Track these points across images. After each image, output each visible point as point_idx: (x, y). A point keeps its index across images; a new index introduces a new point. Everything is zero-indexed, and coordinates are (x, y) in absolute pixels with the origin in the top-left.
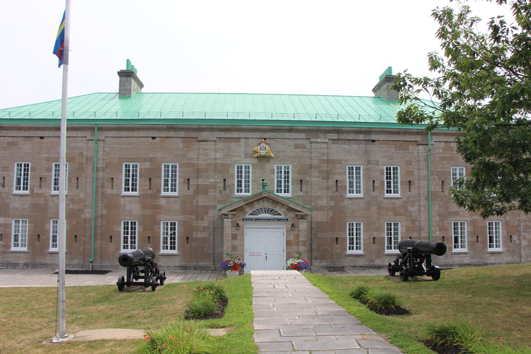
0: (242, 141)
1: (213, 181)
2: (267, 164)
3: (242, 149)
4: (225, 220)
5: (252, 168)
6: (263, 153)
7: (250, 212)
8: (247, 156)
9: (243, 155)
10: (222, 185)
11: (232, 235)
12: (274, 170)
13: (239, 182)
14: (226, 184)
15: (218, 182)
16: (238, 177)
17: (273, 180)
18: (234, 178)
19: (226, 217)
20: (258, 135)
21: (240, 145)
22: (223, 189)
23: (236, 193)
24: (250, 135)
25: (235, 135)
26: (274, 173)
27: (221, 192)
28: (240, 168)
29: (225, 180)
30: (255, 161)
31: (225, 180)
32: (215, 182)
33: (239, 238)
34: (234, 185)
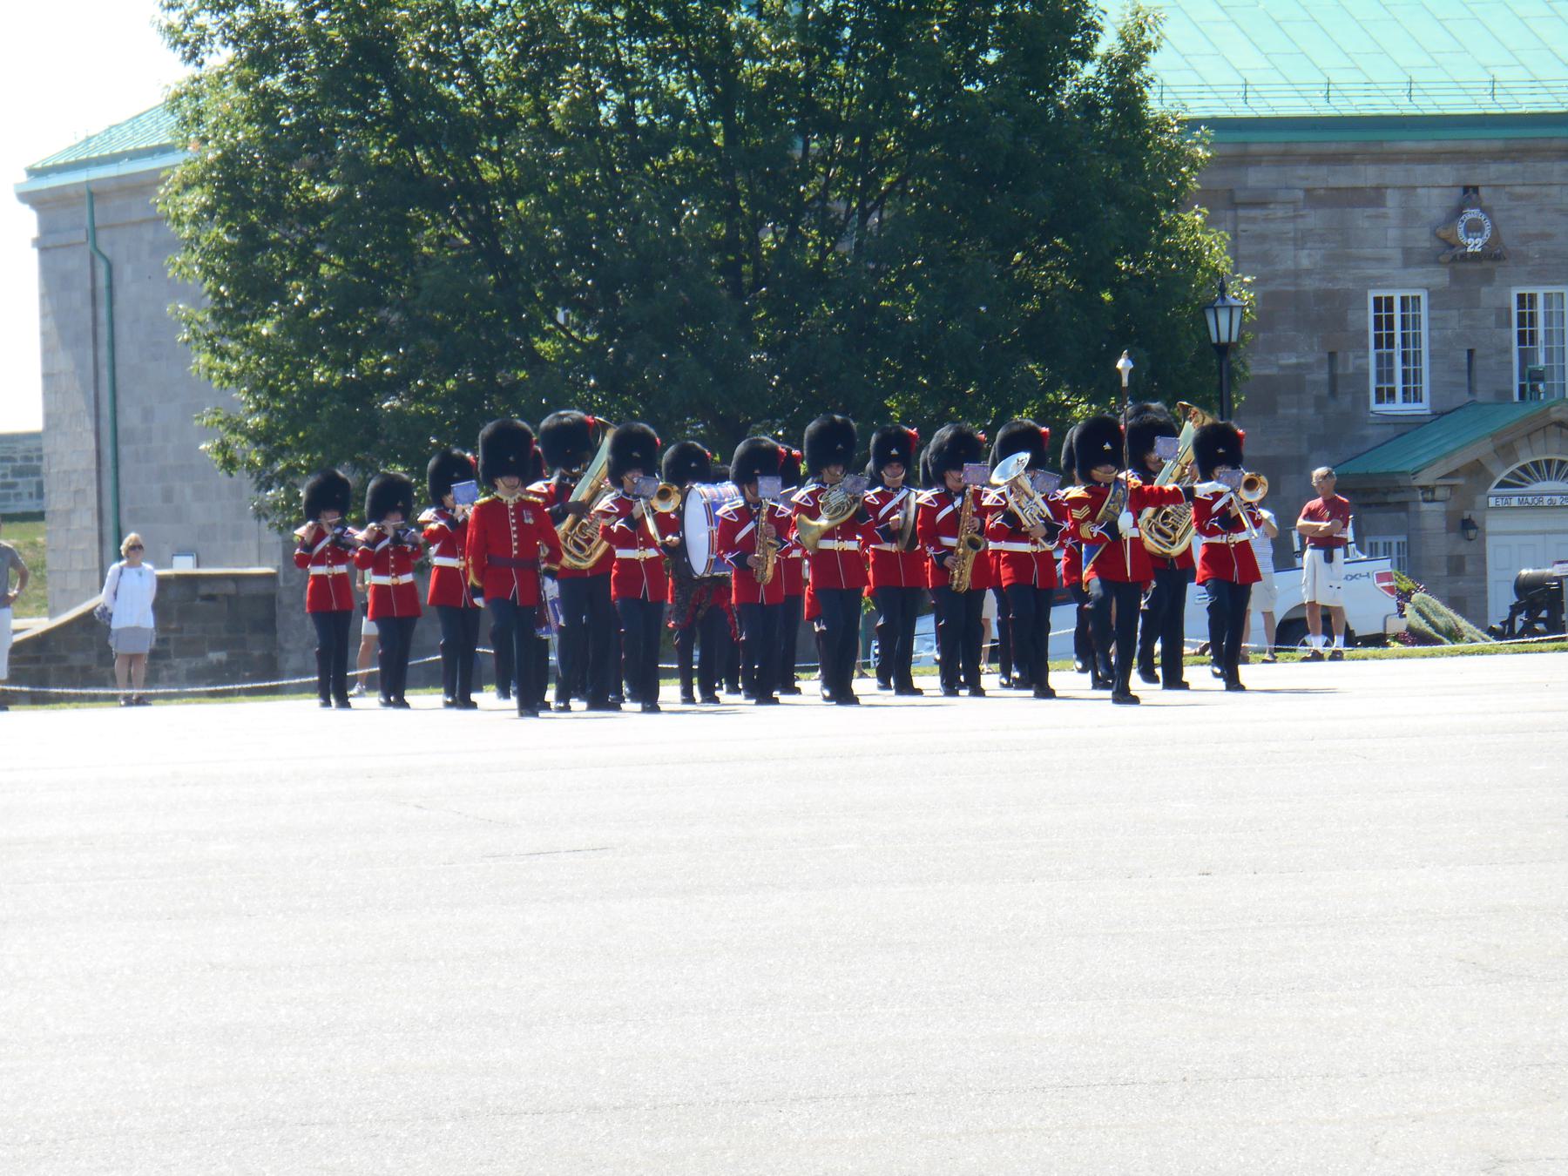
0: (1392, 199)
1: (1293, 361)
2: (1484, 290)
3: (1393, 233)
4: (1425, 507)
5: (1431, 307)
6: (1474, 244)
7: (1502, 476)
8: (1410, 258)
9: (1396, 254)
10: (1322, 375)
11: (1450, 558)
12: (1509, 311)
13: (1385, 363)
14: (1340, 371)
15: (1308, 366)
16: (1378, 345)
17: (1508, 351)
18: (1366, 347)
19: (1429, 496)
20: (1448, 174)
21: (1384, 216)
22: (1325, 391)
23: (1374, 407)
24: (1421, 171)
25: (1368, 175)
26: (1509, 325)
27: (1320, 403)
28: (1383, 304)
29: (1332, 355)
30: (1440, 277)
31: (1332, 355)
32: (1298, 366)
33: (1469, 568)
34: (1367, 375)
